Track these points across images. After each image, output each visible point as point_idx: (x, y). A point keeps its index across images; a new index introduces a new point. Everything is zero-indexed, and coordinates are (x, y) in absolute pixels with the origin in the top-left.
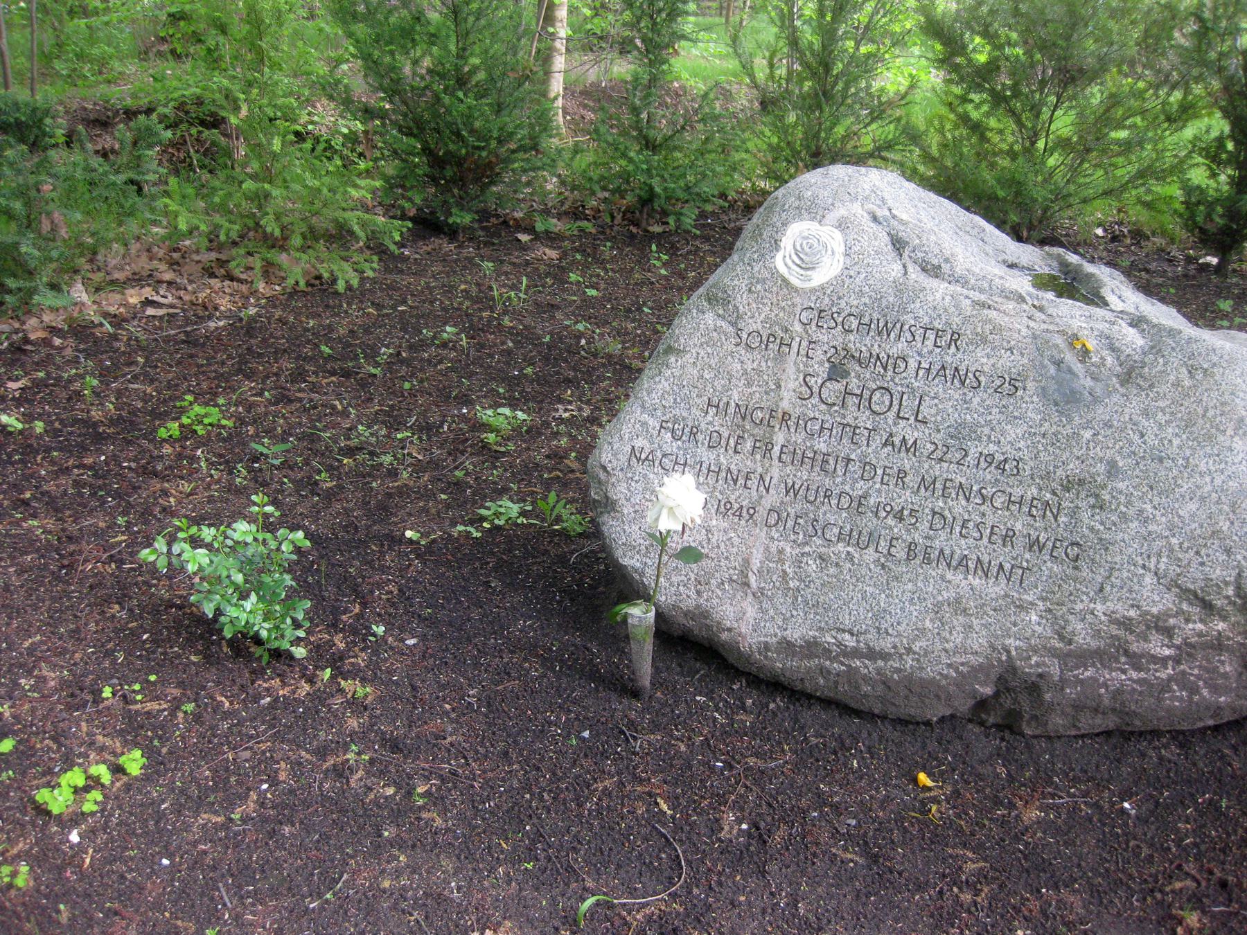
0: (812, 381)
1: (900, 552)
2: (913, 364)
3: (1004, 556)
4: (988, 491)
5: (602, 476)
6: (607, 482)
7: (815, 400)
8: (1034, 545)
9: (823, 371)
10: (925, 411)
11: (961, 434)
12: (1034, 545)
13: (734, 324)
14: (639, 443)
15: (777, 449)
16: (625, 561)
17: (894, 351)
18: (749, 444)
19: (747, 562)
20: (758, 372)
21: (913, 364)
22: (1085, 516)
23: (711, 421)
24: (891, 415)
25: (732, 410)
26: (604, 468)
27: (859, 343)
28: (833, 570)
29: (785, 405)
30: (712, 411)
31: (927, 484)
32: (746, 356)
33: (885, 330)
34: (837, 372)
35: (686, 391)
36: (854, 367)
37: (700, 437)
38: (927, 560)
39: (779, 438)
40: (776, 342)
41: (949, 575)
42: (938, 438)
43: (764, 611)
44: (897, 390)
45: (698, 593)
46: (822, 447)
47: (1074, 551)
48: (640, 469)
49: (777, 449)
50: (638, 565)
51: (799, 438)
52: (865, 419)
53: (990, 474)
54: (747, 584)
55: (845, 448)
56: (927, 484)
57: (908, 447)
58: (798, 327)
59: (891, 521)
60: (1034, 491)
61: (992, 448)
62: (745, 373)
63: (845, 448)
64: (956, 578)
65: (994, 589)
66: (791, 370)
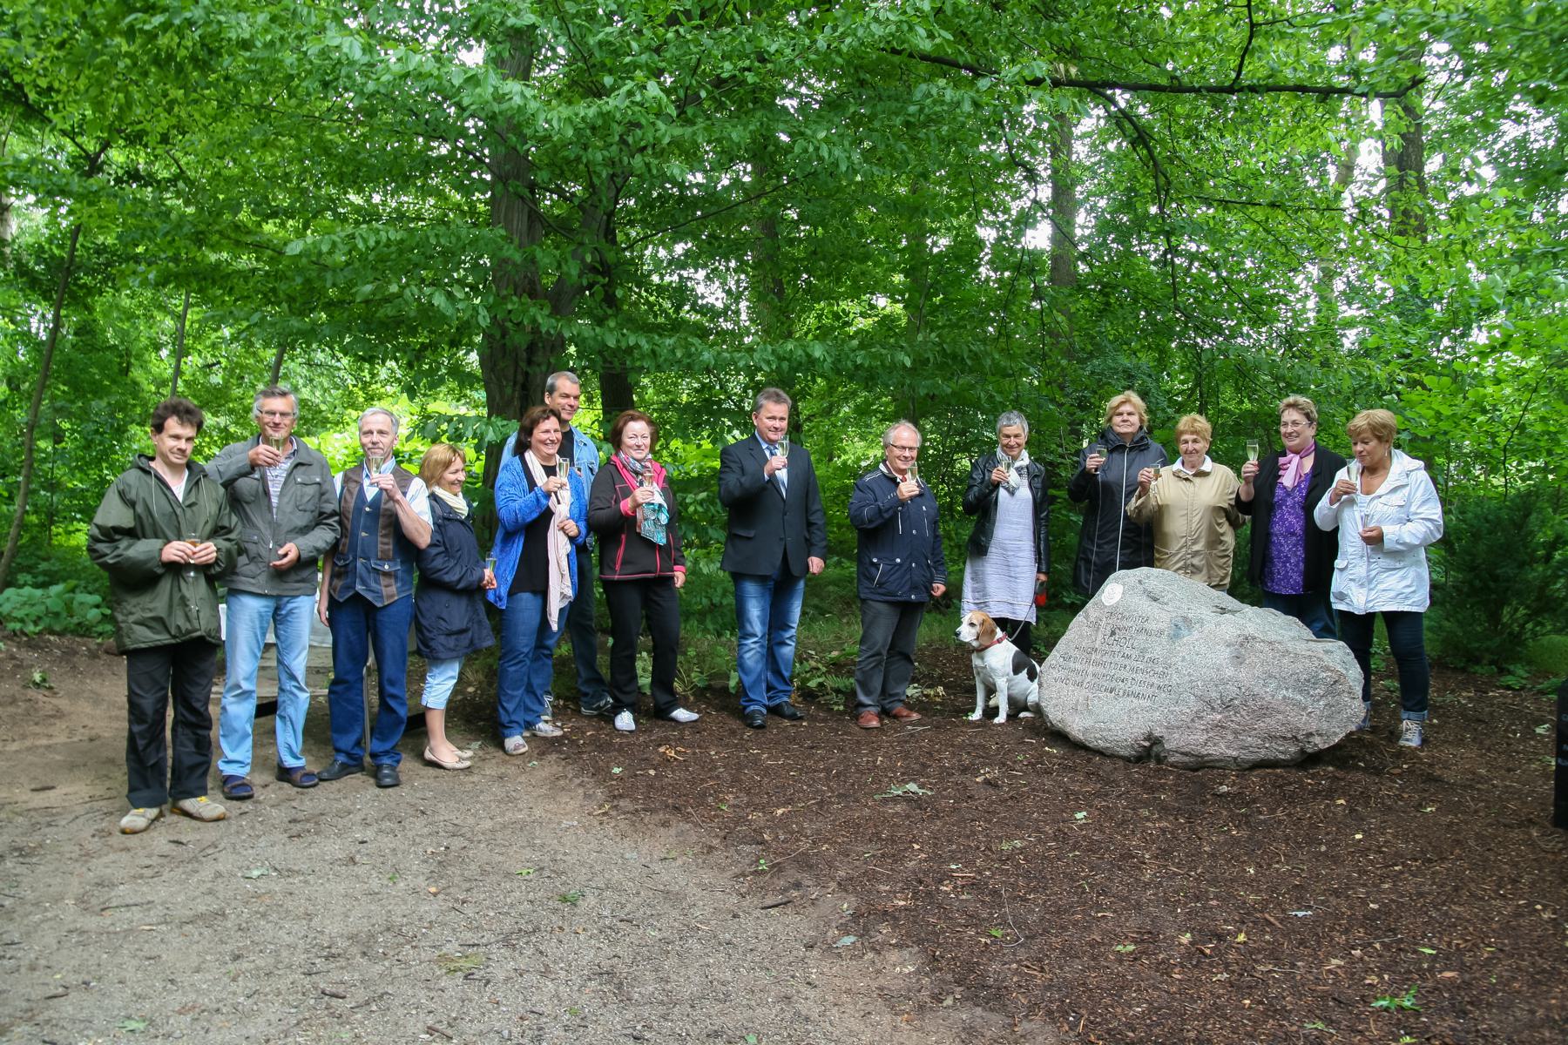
3: (1150, 691)
11: (1144, 651)
23: (1076, 653)
34: (1113, 633)
52: (1117, 649)
57: (1129, 657)
65: (1145, 703)
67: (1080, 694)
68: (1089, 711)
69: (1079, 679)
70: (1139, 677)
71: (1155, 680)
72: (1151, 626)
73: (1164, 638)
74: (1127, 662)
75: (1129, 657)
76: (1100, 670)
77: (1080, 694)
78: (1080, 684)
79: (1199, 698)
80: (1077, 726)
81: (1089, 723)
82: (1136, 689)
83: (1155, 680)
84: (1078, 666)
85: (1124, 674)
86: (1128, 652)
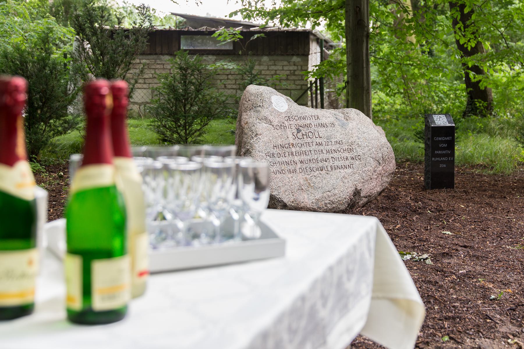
0: (294, 134)
1: (329, 169)
2: (313, 125)
3: (347, 163)
4: (339, 150)
7: (297, 139)
8: (352, 158)
9: (295, 131)
10: (320, 135)
11: (329, 138)
12: (352, 158)
13: (271, 125)
18: (287, 153)
19: (300, 183)
21: (313, 125)
22: (358, 149)
23: (276, 151)
24: (314, 137)
25: (280, 146)
27: (302, 122)
28: (318, 178)
29: (291, 142)
31: (328, 152)
33: (304, 118)
34: (299, 131)
36: (301, 128)
37: (275, 155)
38: (335, 169)
40: (282, 127)
41: (340, 170)
42: (325, 140)
43: (308, 194)
44: (312, 131)
45: (293, 195)
46: (304, 150)
47: (359, 157)
50: (277, 193)
53: (338, 146)
54: (302, 189)
55: (308, 149)
56: (328, 152)
57: (321, 144)
58: (286, 122)
59: (325, 162)
60: (347, 147)
61: (336, 139)
62: (279, 136)
63: (308, 149)
64: (342, 171)
65: (349, 171)
67: (299, 178)
68: (313, 187)
69: (291, 167)
70: (335, 155)
71: (349, 155)
73: (338, 128)
74: (321, 148)
75: (321, 144)
76: (303, 157)
77: (299, 178)
78: (295, 171)
79: (375, 159)
83: (349, 155)
84: (284, 159)
85: (325, 156)
86: (318, 140)
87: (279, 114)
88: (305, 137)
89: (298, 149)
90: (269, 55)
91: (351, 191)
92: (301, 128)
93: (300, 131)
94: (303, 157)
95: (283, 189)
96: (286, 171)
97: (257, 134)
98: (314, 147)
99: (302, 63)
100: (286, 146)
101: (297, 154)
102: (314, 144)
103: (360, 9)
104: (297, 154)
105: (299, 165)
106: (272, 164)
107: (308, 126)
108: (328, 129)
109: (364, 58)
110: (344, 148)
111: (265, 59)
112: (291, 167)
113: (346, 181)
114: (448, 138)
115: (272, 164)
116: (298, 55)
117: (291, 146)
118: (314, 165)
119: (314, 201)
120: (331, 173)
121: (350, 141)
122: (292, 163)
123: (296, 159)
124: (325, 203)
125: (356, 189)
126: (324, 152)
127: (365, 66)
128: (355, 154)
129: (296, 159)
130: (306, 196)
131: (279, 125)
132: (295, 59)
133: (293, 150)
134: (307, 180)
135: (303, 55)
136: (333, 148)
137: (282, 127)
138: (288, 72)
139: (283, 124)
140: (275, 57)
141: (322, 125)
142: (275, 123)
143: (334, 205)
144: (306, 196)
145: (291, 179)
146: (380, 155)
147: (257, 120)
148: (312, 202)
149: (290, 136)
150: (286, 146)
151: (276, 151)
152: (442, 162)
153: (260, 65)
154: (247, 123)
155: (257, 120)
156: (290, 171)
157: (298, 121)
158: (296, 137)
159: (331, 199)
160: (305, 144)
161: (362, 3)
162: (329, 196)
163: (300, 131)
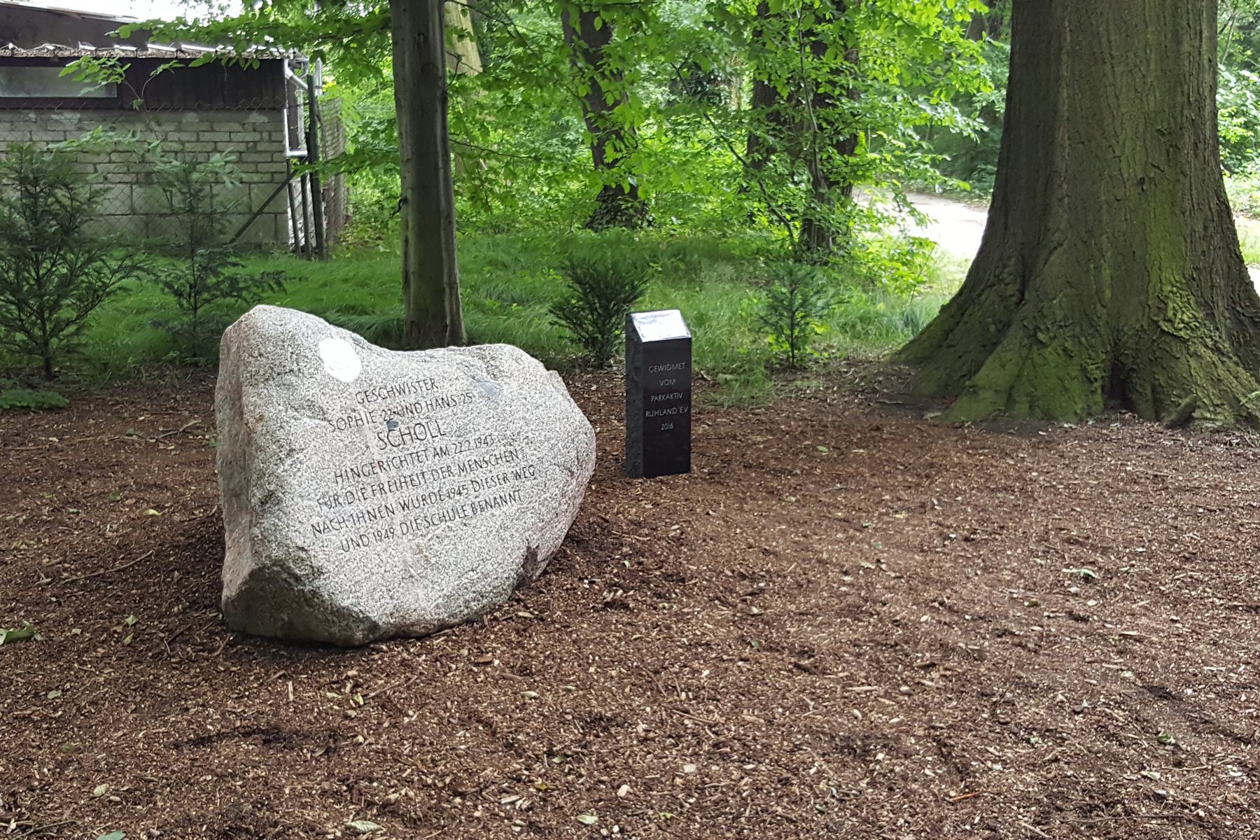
1: (469, 512)
2: (424, 405)
3: (507, 488)
5: (303, 555)
6: (309, 557)
8: (517, 476)
9: (385, 427)
11: (461, 433)
12: (517, 476)
13: (324, 419)
14: (315, 520)
15: (386, 486)
16: (346, 603)
17: (413, 401)
18: (370, 490)
20: (353, 442)
21: (424, 405)
23: (341, 488)
24: (429, 437)
25: (350, 474)
26: (303, 549)
27: (399, 402)
29: (377, 457)
30: (339, 479)
32: (342, 436)
33: (401, 391)
34: (391, 425)
35: (320, 473)
37: (341, 500)
38: (482, 509)
39: (383, 477)
40: (351, 421)
45: (392, 598)
46: (408, 473)
48: (324, 536)
49: (386, 486)
51: (393, 472)
54: (412, 576)
57: (444, 452)
58: (360, 407)
59: (457, 497)
64: (496, 512)
66: (367, 432)
68: (435, 567)
70: (480, 474)
72: (447, 390)
73: (481, 404)
74: (447, 460)
75: (444, 452)
76: (408, 493)
77: (400, 551)
78: (391, 532)
80: (424, 601)
81: (449, 585)
82: (487, 494)
85: (457, 480)
86: (439, 443)
87: (342, 387)
88: (407, 438)
89: (393, 472)
90: (199, 109)
91: (518, 555)
92: (396, 418)
93: (396, 424)
94: (408, 493)
95: (367, 586)
96: (371, 536)
97: (292, 450)
98: (431, 462)
99: (270, 127)
100: (366, 469)
101: (393, 488)
102: (431, 453)
103: (426, 39)
104: (393, 488)
105: (399, 515)
106: (337, 526)
107: (410, 409)
108: (457, 410)
109: (439, 148)
110: (497, 453)
111: (191, 117)
112: (381, 525)
113: (508, 534)
114: (678, 366)
115: (337, 526)
116: (261, 110)
117: (377, 470)
118: (434, 510)
119: (440, 600)
120: (474, 521)
121: (508, 433)
122: (384, 513)
123: (392, 500)
124: (467, 601)
125: (529, 548)
126: (454, 469)
127: (441, 165)
128: (523, 464)
129: (392, 500)
130: (421, 593)
131: (345, 417)
132: (256, 118)
133: (383, 477)
134: (421, 552)
135: (274, 109)
136: (474, 458)
137: (351, 421)
138: (242, 147)
139: (353, 414)
140: (211, 114)
141: (445, 403)
142: (334, 414)
143: (485, 601)
144: (421, 593)
145: (384, 556)
146: (574, 454)
147: (290, 411)
148: (437, 606)
149: (373, 442)
150: (366, 469)
151: (341, 488)
152: (669, 418)
153: (179, 130)
154: (261, 418)
155: (290, 411)
156: (379, 536)
157: (388, 400)
158: (386, 443)
159: (479, 587)
160: (409, 458)
161: (431, 25)
162: (473, 583)
163: (396, 424)
